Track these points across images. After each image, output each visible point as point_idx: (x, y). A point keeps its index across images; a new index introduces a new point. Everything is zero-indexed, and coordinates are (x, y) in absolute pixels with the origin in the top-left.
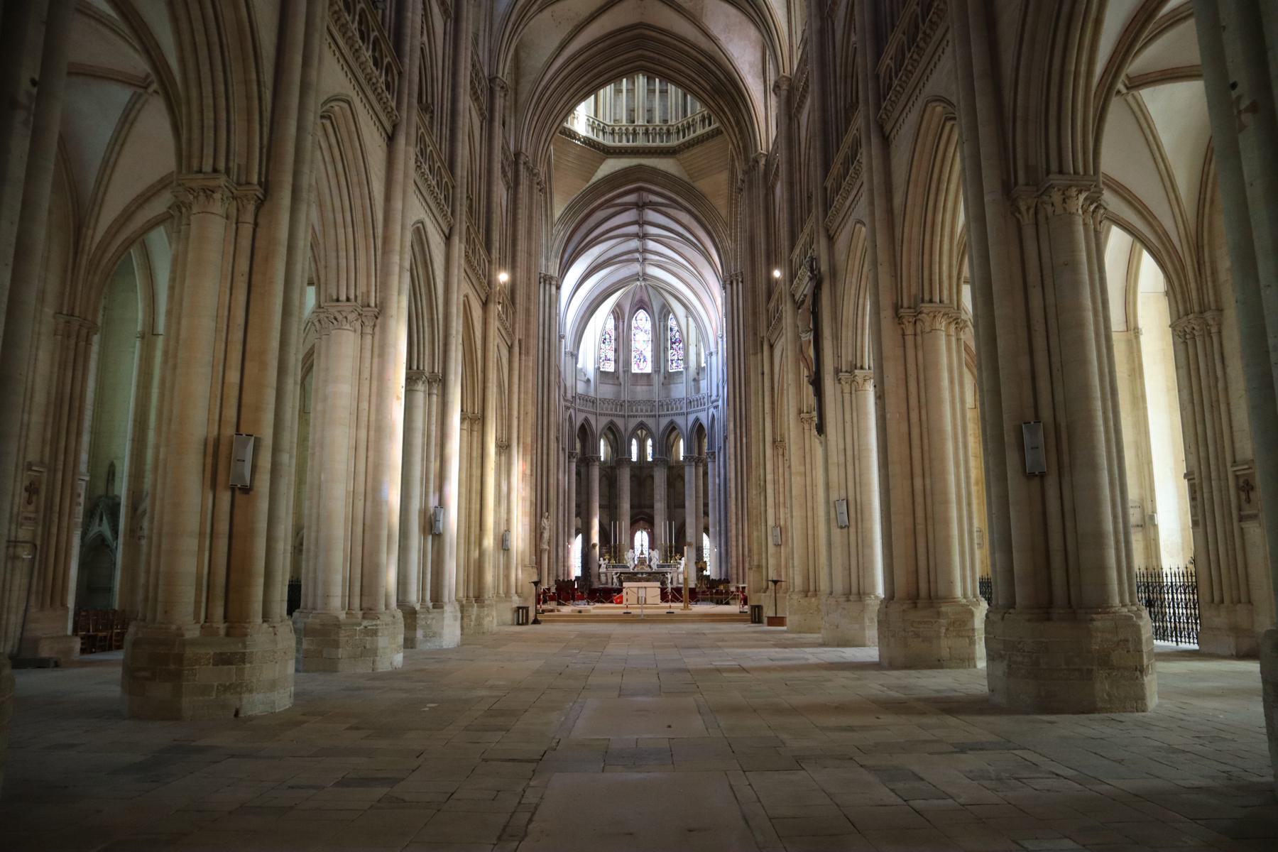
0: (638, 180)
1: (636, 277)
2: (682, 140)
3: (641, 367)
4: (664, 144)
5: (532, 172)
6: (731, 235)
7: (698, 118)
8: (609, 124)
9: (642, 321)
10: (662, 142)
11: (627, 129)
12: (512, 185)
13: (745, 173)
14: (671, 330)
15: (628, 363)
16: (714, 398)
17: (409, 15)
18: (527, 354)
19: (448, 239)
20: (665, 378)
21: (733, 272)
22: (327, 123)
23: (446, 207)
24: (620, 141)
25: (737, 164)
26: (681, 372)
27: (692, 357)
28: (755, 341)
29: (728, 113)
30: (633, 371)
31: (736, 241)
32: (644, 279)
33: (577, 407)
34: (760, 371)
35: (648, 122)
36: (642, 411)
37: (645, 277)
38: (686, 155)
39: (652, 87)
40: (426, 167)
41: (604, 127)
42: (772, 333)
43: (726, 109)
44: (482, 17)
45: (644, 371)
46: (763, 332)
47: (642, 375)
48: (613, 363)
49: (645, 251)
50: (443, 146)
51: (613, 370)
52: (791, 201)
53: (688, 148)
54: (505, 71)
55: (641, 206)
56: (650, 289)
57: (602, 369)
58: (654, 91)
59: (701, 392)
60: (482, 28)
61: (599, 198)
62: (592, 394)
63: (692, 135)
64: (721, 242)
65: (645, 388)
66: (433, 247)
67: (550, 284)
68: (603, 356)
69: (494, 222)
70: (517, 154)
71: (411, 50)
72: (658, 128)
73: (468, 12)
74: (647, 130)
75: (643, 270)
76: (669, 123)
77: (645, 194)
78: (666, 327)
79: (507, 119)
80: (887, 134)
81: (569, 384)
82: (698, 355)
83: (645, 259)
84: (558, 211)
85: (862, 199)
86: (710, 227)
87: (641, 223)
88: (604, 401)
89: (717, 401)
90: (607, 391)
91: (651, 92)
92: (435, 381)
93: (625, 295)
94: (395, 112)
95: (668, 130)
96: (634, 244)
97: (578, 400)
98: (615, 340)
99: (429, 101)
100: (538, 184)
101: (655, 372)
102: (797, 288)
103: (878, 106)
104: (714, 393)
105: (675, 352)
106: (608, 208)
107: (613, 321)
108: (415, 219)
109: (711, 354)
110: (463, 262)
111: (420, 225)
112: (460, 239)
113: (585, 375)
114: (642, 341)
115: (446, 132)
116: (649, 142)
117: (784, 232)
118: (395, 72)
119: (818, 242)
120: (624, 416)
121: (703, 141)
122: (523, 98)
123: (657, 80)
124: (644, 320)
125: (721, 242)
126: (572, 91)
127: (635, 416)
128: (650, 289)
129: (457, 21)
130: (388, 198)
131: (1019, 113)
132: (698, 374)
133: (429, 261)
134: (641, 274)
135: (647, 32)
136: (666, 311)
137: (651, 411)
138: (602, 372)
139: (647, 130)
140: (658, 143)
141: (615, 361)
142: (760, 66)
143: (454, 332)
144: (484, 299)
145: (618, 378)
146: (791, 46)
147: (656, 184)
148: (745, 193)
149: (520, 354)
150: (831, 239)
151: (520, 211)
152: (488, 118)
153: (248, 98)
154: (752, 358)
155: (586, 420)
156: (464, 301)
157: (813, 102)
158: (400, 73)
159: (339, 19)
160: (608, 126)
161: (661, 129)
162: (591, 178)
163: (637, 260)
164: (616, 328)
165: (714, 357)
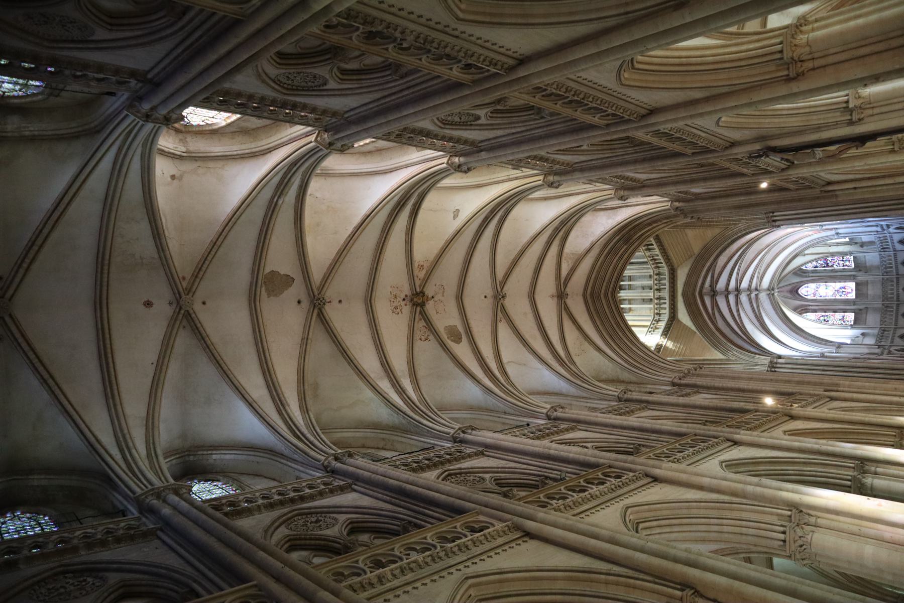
0: (694, 295)
1: (771, 296)
2: (664, 265)
3: (850, 291)
4: (667, 277)
5: (687, 374)
6: (736, 224)
7: (648, 253)
9: (808, 290)
11: (657, 304)
12: (696, 389)
13: (686, 217)
14: (816, 267)
15: (847, 302)
16: (879, 229)
17: (571, 455)
18: (837, 385)
19: (736, 443)
20: (860, 271)
21: (765, 220)
22: (641, 526)
23: (710, 442)
24: (665, 309)
25: (678, 223)
26: (855, 258)
28: (824, 198)
29: (643, 232)
30: (854, 297)
31: (739, 220)
32: (773, 289)
33: (889, 344)
34: (852, 191)
35: (651, 289)
36: (892, 290)
37: (770, 289)
38: (674, 260)
39: (627, 287)
40: (679, 455)
42: (817, 184)
43: (640, 233)
44: (578, 403)
45: (854, 288)
46: (816, 192)
47: (857, 290)
48: (846, 314)
49: (749, 289)
50: (665, 439)
51: (853, 314)
52: (705, 179)
53: (669, 260)
54: (613, 390)
55: (714, 293)
56: (780, 285)
57: (852, 323)
58: (630, 285)
59: (873, 240)
60: (586, 404)
61: (707, 324)
62: (876, 331)
63: (660, 257)
64: (740, 231)
65: (870, 287)
66: (742, 456)
67: (776, 363)
68: (840, 322)
69: (724, 405)
70: (674, 384)
71: (595, 457)
72: (656, 282)
73: (573, 414)
74: (657, 290)
75: (765, 290)
76: (652, 274)
77: (704, 291)
78: (813, 272)
79: (648, 390)
80: (648, 111)
81: (866, 351)
82: (838, 244)
83: (756, 290)
84: (717, 355)
85: (699, 123)
86: (729, 241)
87: (727, 293)
88: (882, 321)
89: (882, 226)
90: (873, 319)
91: (630, 287)
92: (862, 467)
93: (786, 304)
94: (636, 474)
95: (657, 274)
96: (744, 298)
97: (882, 343)
98: (825, 312)
99: (632, 446)
100: (696, 370)
101: (854, 279)
102: (776, 167)
103: (628, 121)
104: (875, 229)
105: (836, 264)
106: (715, 318)
107: (808, 314)
108: (718, 468)
109: (837, 234)
110: (755, 433)
111: (724, 464)
112: (736, 433)
113: (858, 337)
114: (827, 291)
115: (653, 436)
117: (730, 182)
118: (608, 470)
119: (736, 154)
120: (898, 305)
121: (664, 249)
122: (633, 378)
123: (622, 283)
124: (807, 289)
125: (740, 231)
126: (628, 343)
127: (898, 296)
128: (780, 285)
129: (578, 421)
130: (701, 488)
131: (622, 11)
132: (856, 243)
133: (754, 460)
134: (768, 292)
135: (589, 291)
136: (800, 272)
137: (893, 281)
138: (855, 323)
139: (657, 290)
140: (666, 282)
141: (844, 312)
142: (609, 211)
143: (816, 447)
144: (787, 418)
145: (860, 310)
146: (594, 191)
147: (697, 282)
148: (701, 216)
150: (733, 144)
151: (717, 385)
152: (646, 404)
153: (617, 584)
154: (840, 199)
156: (789, 435)
157: (631, 171)
158: (610, 467)
159: (570, 506)
162: (693, 330)
163: (757, 295)
164: (814, 311)
165: (840, 231)
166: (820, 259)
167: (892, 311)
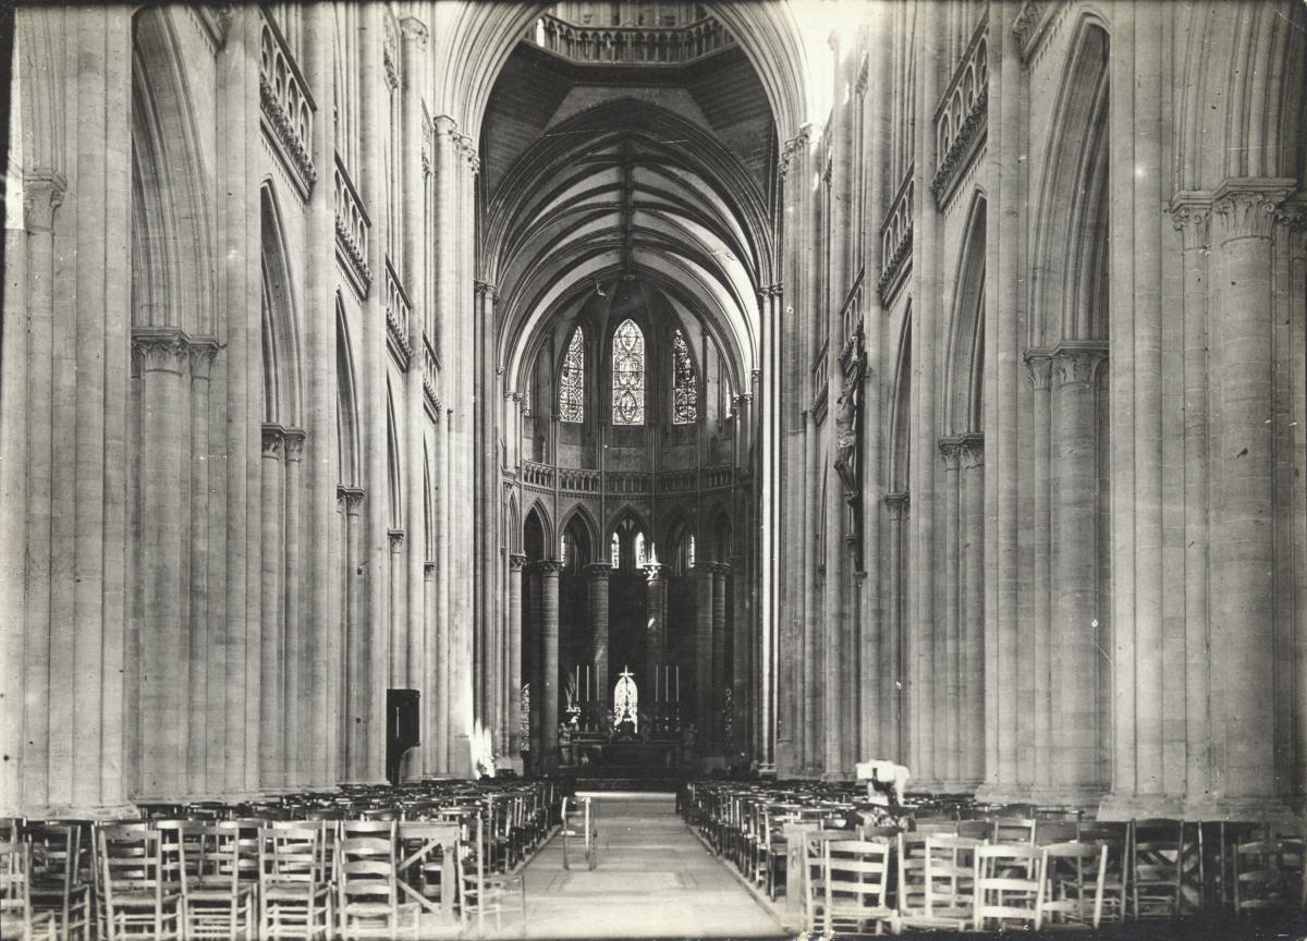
6: (772, 222)
8: (577, 25)
9: (630, 336)
10: (664, 59)
11: (607, 35)
27: (712, 401)
41: (568, 32)
63: (713, 51)
74: (640, 36)
95: (674, 37)
116: (642, 58)
149: (449, 429)
154: (790, 439)
155: (538, 503)
160: (576, 29)
161: (663, 37)
162: (547, 121)
166: (694, 363)
167: (586, 488)
